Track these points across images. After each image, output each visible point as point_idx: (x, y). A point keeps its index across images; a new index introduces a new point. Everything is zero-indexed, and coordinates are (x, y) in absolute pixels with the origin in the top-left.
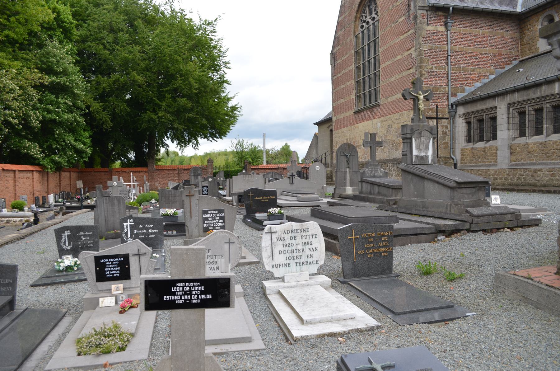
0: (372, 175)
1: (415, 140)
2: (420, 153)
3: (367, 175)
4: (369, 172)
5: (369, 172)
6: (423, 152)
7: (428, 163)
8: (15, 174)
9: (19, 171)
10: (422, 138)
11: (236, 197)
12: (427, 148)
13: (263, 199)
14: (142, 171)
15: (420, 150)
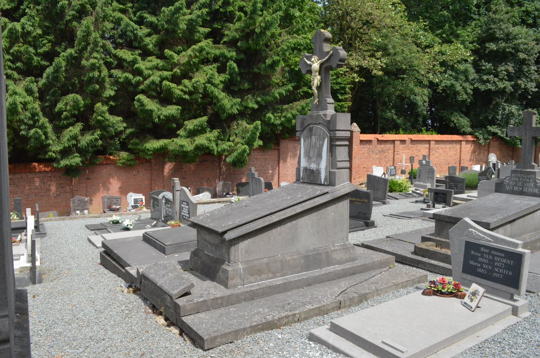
0: (516, 189)
1: (305, 140)
2: (310, 163)
3: (507, 188)
4: (511, 183)
5: (511, 183)
6: (314, 162)
7: (319, 183)
10: (313, 138)
11: (432, 194)
12: (320, 156)
13: (356, 201)
15: (310, 158)
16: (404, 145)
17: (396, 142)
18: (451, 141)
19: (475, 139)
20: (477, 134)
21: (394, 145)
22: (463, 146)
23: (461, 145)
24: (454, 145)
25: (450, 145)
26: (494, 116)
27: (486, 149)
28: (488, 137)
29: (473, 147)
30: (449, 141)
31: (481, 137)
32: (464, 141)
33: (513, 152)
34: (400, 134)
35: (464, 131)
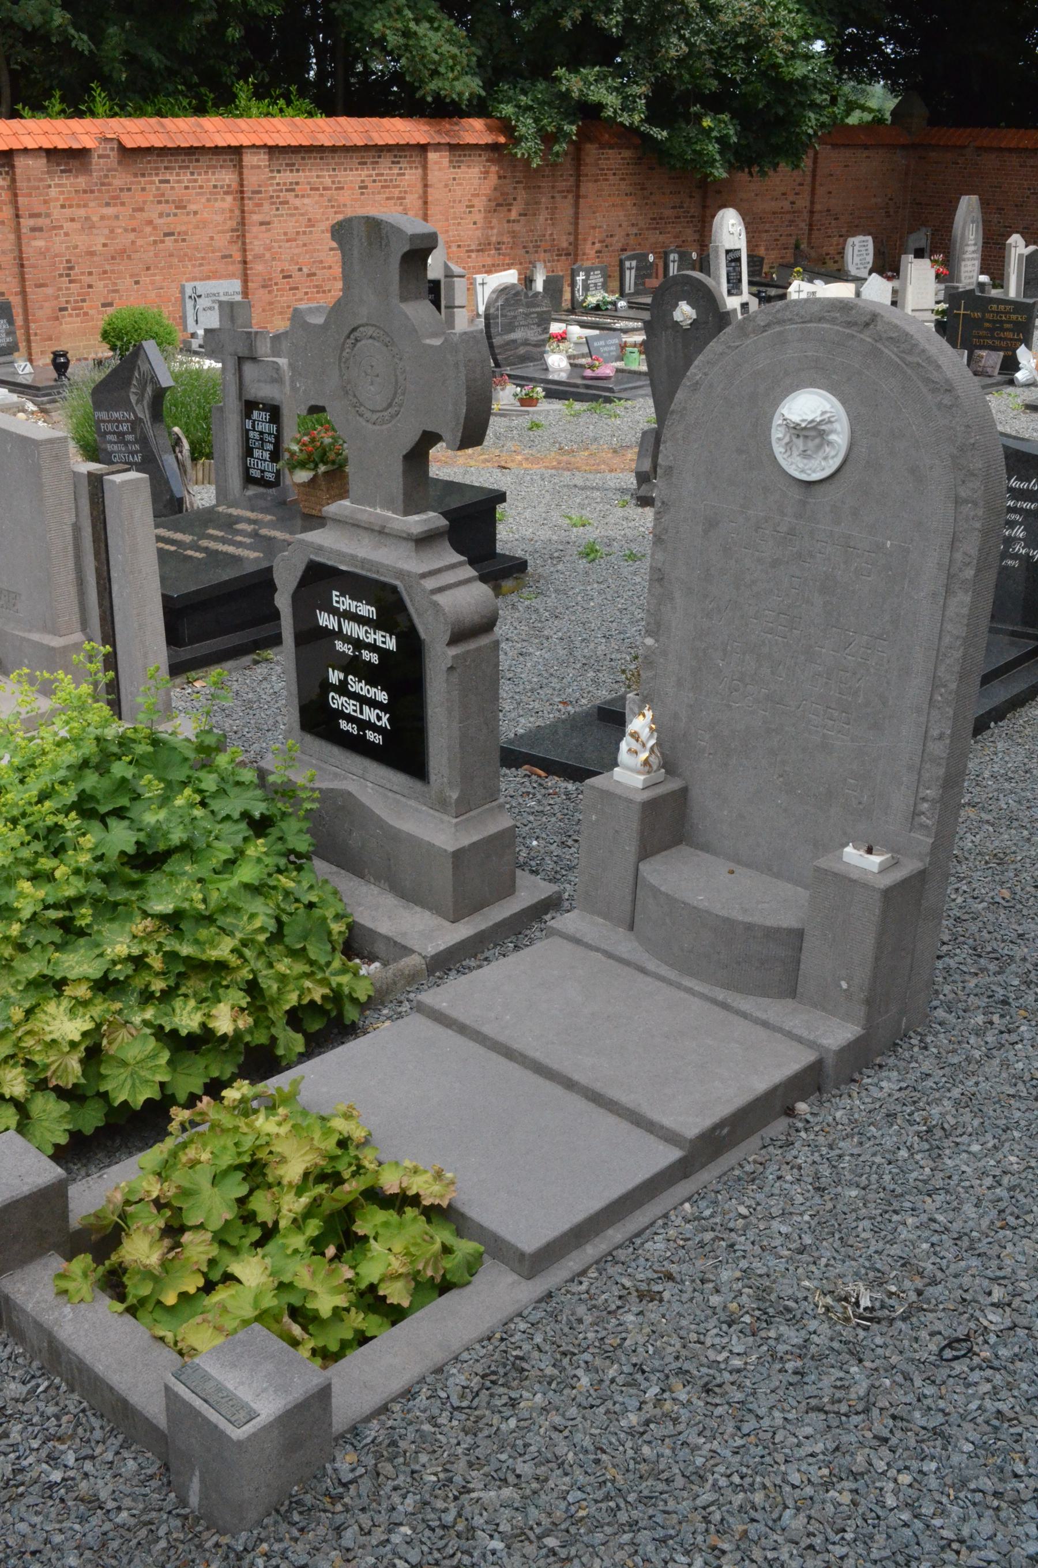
8: (239, 167)
9: (273, 150)
16: (82, 181)
17: (20, 162)
18: (366, 148)
19: (502, 140)
20: (508, 110)
21: (13, 180)
22: (433, 176)
23: (425, 168)
24: (386, 168)
25: (364, 174)
26: (586, 16)
27: (562, 185)
28: (560, 129)
29: (493, 179)
30: (355, 148)
31: (526, 126)
32: (438, 147)
33: (704, 198)
34: (93, 114)
35: (437, 97)
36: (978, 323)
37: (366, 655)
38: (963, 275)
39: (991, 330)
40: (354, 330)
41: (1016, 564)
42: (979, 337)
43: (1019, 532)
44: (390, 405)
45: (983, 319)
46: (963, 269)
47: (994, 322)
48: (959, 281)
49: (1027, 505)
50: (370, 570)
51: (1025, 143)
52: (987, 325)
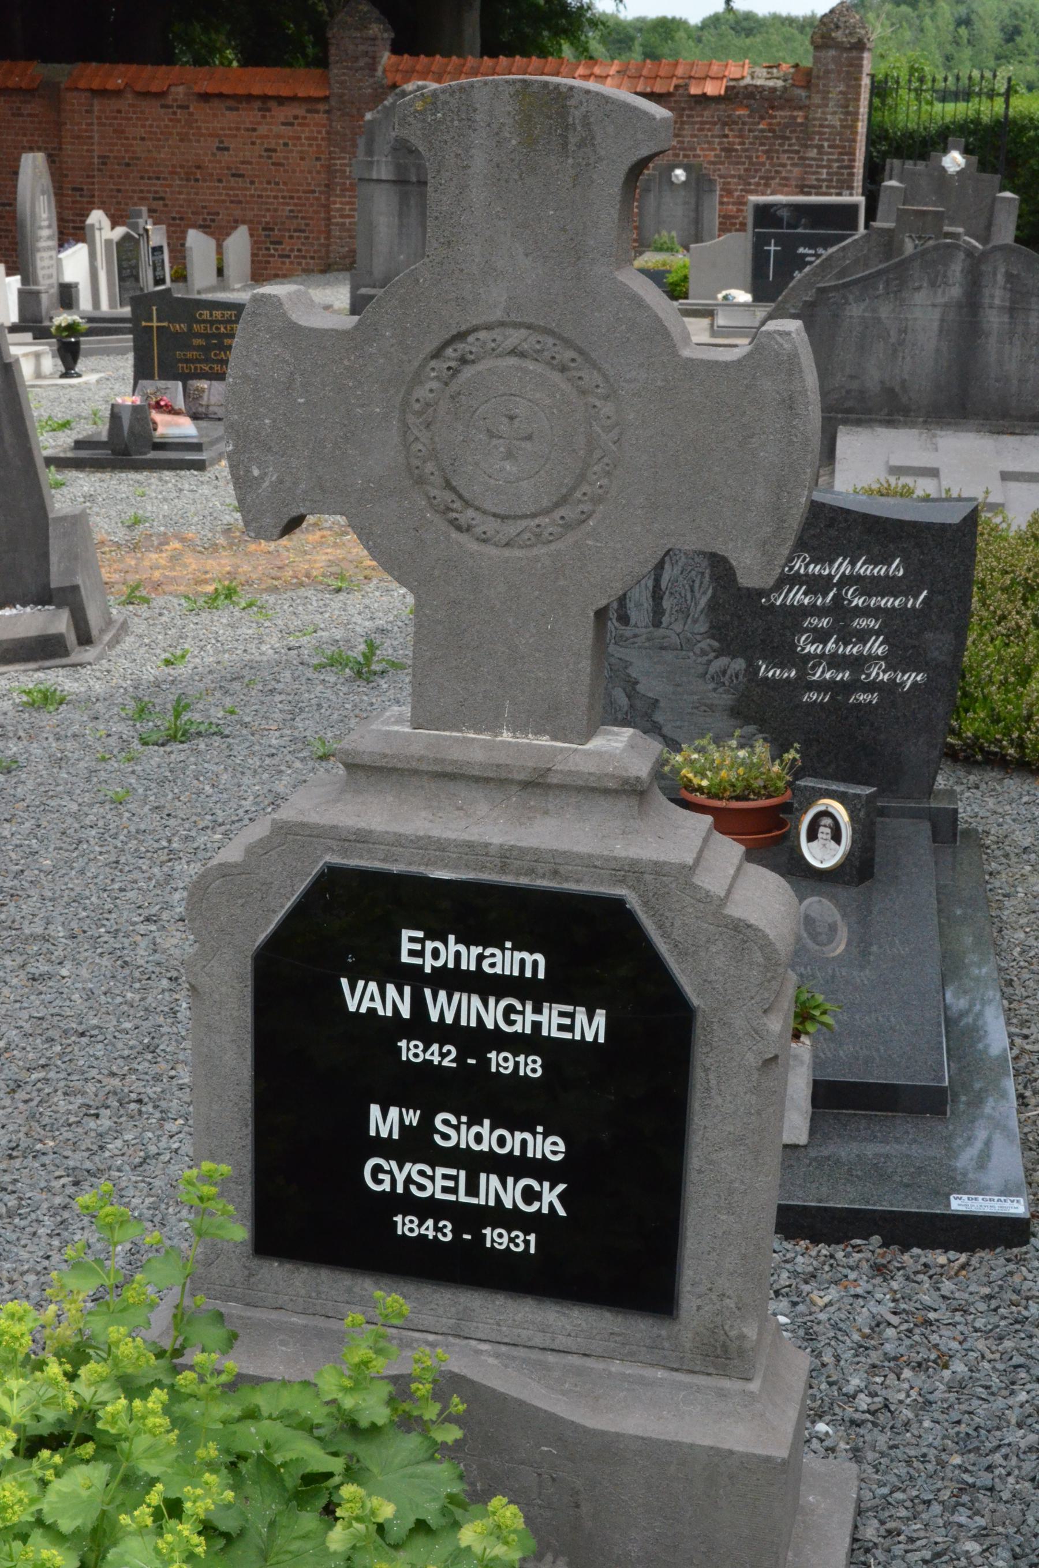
14: (281, 100)
36: (181, 341)
37: (501, 1062)
38: (41, 273)
39: (206, 349)
40: (461, 336)
41: (874, 698)
42: (187, 361)
43: (877, 647)
44: (563, 501)
45: (191, 334)
46: (39, 264)
47: (206, 336)
48: (36, 283)
49: (887, 602)
50: (531, 872)
51: (14, 81)
52: (197, 342)
